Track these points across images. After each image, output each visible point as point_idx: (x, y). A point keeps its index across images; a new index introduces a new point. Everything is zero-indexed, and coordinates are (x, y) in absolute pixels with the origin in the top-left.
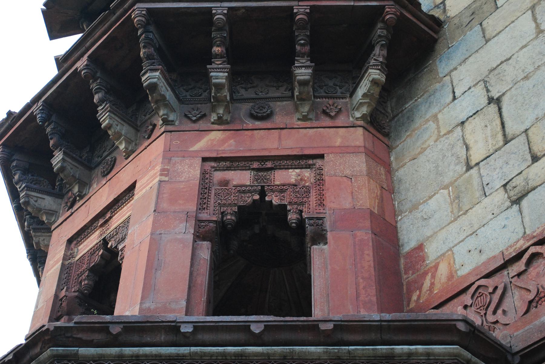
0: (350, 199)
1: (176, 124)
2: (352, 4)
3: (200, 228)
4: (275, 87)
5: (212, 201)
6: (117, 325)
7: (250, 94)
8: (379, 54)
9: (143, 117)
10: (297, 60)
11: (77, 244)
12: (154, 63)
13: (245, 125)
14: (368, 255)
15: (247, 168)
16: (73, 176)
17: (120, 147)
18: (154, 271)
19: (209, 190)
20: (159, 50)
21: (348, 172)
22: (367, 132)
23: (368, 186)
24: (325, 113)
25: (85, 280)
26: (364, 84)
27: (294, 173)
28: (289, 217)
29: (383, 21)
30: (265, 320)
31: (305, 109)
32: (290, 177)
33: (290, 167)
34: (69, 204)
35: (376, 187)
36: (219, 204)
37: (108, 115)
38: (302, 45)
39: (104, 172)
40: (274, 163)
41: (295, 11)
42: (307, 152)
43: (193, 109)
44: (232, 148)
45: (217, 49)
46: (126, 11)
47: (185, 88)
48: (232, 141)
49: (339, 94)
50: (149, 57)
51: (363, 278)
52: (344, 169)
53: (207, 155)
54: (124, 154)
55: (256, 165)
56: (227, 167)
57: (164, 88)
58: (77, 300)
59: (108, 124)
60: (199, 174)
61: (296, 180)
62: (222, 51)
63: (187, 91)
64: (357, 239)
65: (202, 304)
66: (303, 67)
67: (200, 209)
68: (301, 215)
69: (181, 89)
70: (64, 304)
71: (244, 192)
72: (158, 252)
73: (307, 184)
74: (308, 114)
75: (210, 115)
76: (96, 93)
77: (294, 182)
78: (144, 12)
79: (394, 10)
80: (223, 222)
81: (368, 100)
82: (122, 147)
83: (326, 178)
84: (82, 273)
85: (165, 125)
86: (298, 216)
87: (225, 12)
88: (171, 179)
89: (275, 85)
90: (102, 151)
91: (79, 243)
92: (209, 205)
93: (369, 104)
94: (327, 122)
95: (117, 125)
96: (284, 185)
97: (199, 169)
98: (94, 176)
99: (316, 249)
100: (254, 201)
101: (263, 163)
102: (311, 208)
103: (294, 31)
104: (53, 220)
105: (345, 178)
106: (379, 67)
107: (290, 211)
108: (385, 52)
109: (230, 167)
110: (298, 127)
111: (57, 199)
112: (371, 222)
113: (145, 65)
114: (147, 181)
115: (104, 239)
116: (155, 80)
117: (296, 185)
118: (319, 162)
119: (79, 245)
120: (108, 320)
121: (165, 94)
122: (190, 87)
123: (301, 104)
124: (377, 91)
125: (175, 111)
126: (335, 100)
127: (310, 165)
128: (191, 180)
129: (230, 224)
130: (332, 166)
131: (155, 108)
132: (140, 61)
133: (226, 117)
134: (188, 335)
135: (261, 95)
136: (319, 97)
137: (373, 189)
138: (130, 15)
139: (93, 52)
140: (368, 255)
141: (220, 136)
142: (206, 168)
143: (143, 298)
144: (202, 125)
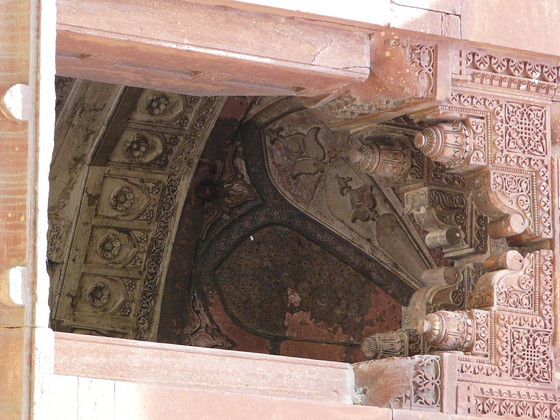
3: (413, 50)
5: (504, 93)
68: (456, 348)
71: (534, 189)
86: (452, 340)
92: (487, 81)
100: (505, 218)
102: (475, 378)
107: (471, 316)
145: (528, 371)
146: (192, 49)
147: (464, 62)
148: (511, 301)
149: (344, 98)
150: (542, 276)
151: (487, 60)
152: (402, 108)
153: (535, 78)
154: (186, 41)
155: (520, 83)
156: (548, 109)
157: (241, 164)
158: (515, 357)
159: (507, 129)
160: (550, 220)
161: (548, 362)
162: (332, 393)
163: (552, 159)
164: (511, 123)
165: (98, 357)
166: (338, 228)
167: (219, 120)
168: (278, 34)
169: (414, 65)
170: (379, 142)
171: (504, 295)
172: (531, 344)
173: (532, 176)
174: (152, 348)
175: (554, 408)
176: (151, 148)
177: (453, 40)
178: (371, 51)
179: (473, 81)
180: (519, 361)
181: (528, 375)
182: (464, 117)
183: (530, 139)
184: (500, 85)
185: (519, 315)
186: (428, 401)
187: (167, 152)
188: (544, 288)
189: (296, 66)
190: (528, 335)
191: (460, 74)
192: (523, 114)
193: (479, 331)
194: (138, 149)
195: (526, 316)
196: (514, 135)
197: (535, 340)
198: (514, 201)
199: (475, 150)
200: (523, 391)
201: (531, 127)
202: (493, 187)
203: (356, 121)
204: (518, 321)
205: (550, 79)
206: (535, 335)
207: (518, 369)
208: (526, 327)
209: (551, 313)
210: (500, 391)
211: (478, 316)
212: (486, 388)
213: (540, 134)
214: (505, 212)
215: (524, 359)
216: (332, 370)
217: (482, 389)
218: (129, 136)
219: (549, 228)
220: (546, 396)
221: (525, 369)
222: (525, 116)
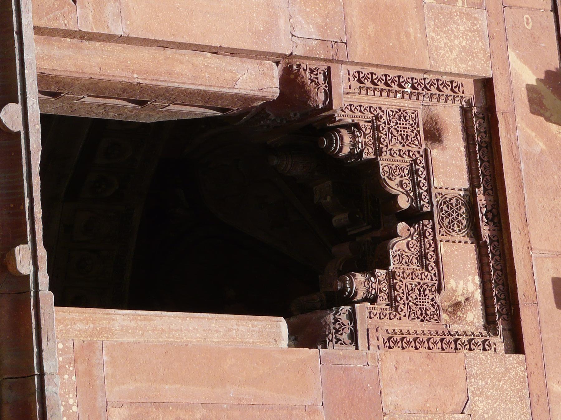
3: (312, 71)
32: (461, 278)
36: (378, 118)
44: (523, 147)
52: (488, 397)
65: (125, 74)
80: (336, 129)
92: (370, 93)
96: (437, 263)
99: (279, 327)
105: (463, 398)
128: (430, 53)
145: (421, 314)
146: (141, 81)
147: (352, 79)
148: (404, 262)
153: (408, 89)
154: (135, 76)
155: (396, 92)
158: (411, 304)
159: (389, 129)
163: (426, 150)
164: (392, 124)
171: (398, 257)
175: (444, 341)
180: (414, 307)
181: (421, 318)
190: (419, 287)
191: (350, 88)
192: (400, 117)
193: (381, 286)
196: (395, 133)
197: (424, 290)
201: (408, 126)
206: (425, 286)
207: (414, 313)
209: (435, 269)
211: (379, 274)
213: (415, 132)
215: (417, 305)
222: (402, 118)
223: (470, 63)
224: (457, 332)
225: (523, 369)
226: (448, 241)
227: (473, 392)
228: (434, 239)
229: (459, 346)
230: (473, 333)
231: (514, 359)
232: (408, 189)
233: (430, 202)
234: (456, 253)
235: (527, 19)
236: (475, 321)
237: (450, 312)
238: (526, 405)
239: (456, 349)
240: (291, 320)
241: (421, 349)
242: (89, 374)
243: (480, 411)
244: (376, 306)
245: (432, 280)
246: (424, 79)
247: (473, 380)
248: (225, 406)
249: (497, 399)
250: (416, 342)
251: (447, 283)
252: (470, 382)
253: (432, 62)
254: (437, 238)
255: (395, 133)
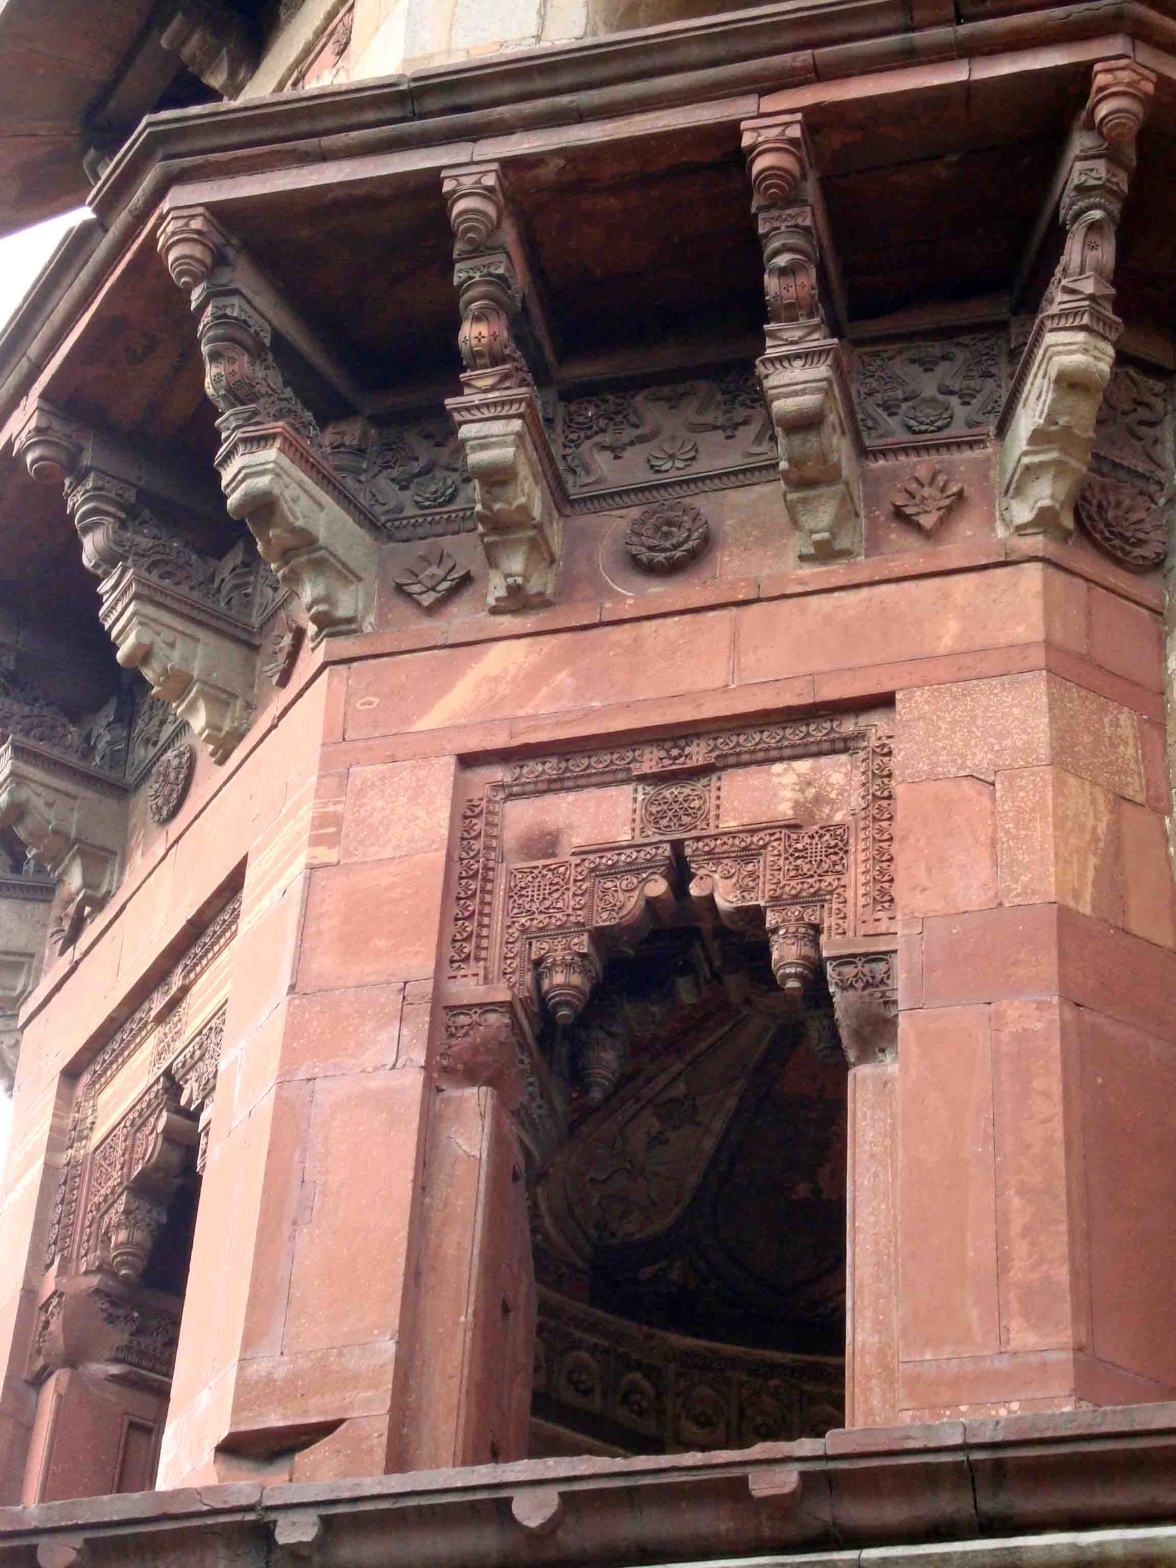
0: (984, 870)
1: (368, 628)
2: (962, 76)
3: (452, 1035)
4: (722, 428)
5: (498, 921)
6: (61, 1538)
7: (630, 469)
8: (1083, 265)
9: (270, 592)
10: (773, 335)
11: (94, 1083)
12: (255, 413)
13: (608, 605)
14: (1046, 1094)
15: (620, 776)
16: (56, 832)
17: (192, 723)
18: (286, 1229)
19: (485, 880)
20: (281, 351)
21: (980, 758)
22: (1060, 578)
23: (1055, 806)
24: (899, 515)
25: (118, 1226)
26: (1035, 392)
27: (790, 778)
28: (775, 955)
29: (1090, 125)
30: (562, 1474)
31: (821, 516)
32: (775, 795)
33: (774, 754)
34: (66, 925)
35: (1094, 802)
36: (524, 930)
37: (134, 614)
38: (783, 272)
39: (159, 809)
40: (715, 748)
41: (747, 140)
42: (830, 692)
43: (425, 560)
44: (566, 704)
45: (475, 333)
46: (141, 218)
47: (395, 473)
48: (563, 677)
49: (958, 429)
50: (239, 393)
51: (1023, 1192)
52: (967, 745)
53: (475, 743)
54: (211, 747)
55: (650, 761)
56: (550, 781)
57: (304, 500)
58: (99, 1305)
59: (138, 646)
60: (446, 823)
61: (796, 804)
62: (494, 336)
63: (403, 488)
64: (1005, 1037)
65: (460, 1335)
66: (798, 356)
67: (452, 962)
68: (816, 944)
69: (382, 481)
70: (56, 1325)
71: (613, 872)
72: (304, 1151)
73: (838, 817)
74: (834, 536)
75: (486, 579)
76: (87, 530)
77: (790, 813)
78: (196, 224)
79: (1125, 76)
80: (542, 998)
81: (1054, 455)
82: (199, 721)
83: (899, 789)
84: (109, 1202)
85: (325, 636)
86: (807, 951)
87: (490, 180)
88: (348, 853)
89: (720, 421)
90: (156, 721)
91: (100, 1080)
92: (484, 943)
93: (1058, 467)
94: (909, 553)
95: (172, 645)
96: (753, 832)
97: (447, 802)
98: (133, 821)
101: (675, 752)
102: (851, 917)
103: (756, 215)
104: (20, 988)
105: (966, 783)
106: (1086, 320)
107: (775, 931)
108: (1106, 253)
109: (560, 780)
110: (800, 589)
111: (29, 906)
112: (1062, 956)
113: (228, 423)
114: (276, 862)
115: (168, 1073)
116: (263, 482)
117: (796, 827)
118: (877, 724)
119: (101, 1091)
120: (34, 1524)
121: (310, 527)
122: (416, 467)
123: (804, 501)
124: (1084, 412)
125: (359, 579)
126: (945, 456)
127: (845, 740)
129: (568, 1004)
130: (922, 735)
131: (284, 577)
132: (208, 410)
133: (541, 582)
134: (305, 1552)
135: (673, 470)
136: (884, 453)
137: (1076, 816)
138: (152, 238)
139: (54, 378)
140: (1046, 1094)
141: (521, 659)
142: (475, 795)
143: (250, 1340)
144: (461, 619)
145: (836, 853)
146: (471, 1310)
147: (462, 972)
148: (751, 884)
149: (520, 1115)
150: (717, 850)
151: (458, 945)
152: (527, 1043)
154: (462, 1319)
156: (513, 866)
157: (646, 1272)
159: (541, 912)
160: (648, 849)
161: (822, 832)
162: (887, 1090)
163: (574, 854)
164: (534, 909)
165: (871, 1389)
166: (709, 1145)
167: (592, 1304)
168: (446, 1204)
169: (471, 1033)
170: (577, 1076)
171: (745, 894)
172: (802, 854)
173: (597, 876)
174: (853, 1321)
175: (878, 816)
176: (634, 1387)
177: (437, 987)
178: (458, 1088)
179: (485, 959)
180: (825, 866)
181: (841, 854)
182: (531, 966)
183: (551, 884)
184: (488, 926)
185: (768, 872)
186: (884, 970)
187: (639, 1367)
188: (732, 846)
189: (483, 1179)
190: (791, 859)
193: (793, 918)
194: (638, 1403)
195: (768, 863)
196: (547, 903)
197: (796, 850)
198: (628, 894)
199: (570, 948)
200: (862, 856)
201: (536, 884)
202: (613, 922)
203: (550, 1103)
204: (776, 873)
205: (475, 867)
207: (835, 865)
208: (781, 862)
209: (761, 834)
210: (864, 884)
212: (862, 901)
213: (544, 872)
214: (643, 903)
216: (858, 1091)
217: (864, 906)
218: (623, 1414)
219: (657, 848)
220: (864, 829)
221: (834, 858)
222: (524, 892)
223: (435, 789)
224: (863, 797)
225: (919, 693)
226: (718, 816)
227: (959, 770)
228: (715, 837)
229: (886, 794)
230: (864, 773)
231: (904, 707)
232: (635, 881)
233: (656, 845)
234: (736, 803)
235: (363, 704)
236: (843, 770)
237: (830, 811)
238: (978, 686)
239: (890, 797)
240: (852, 1060)
241: (893, 851)
242: (957, 1381)
243: (990, 756)
244: (825, 925)
245: (779, 839)
246: (461, 859)
247: (940, 769)
248: (999, 1159)
249: (969, 731)
250: (884, 860)
251: (785, 814)
252: (944, 773)
253: (434, 847)
254: (713, 832)
255: (547, 903)
